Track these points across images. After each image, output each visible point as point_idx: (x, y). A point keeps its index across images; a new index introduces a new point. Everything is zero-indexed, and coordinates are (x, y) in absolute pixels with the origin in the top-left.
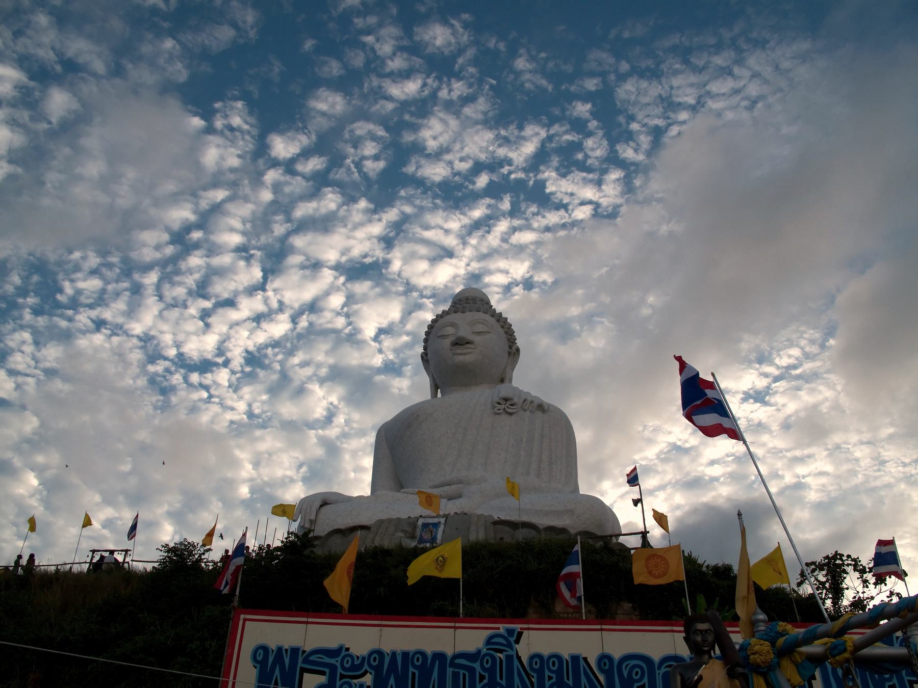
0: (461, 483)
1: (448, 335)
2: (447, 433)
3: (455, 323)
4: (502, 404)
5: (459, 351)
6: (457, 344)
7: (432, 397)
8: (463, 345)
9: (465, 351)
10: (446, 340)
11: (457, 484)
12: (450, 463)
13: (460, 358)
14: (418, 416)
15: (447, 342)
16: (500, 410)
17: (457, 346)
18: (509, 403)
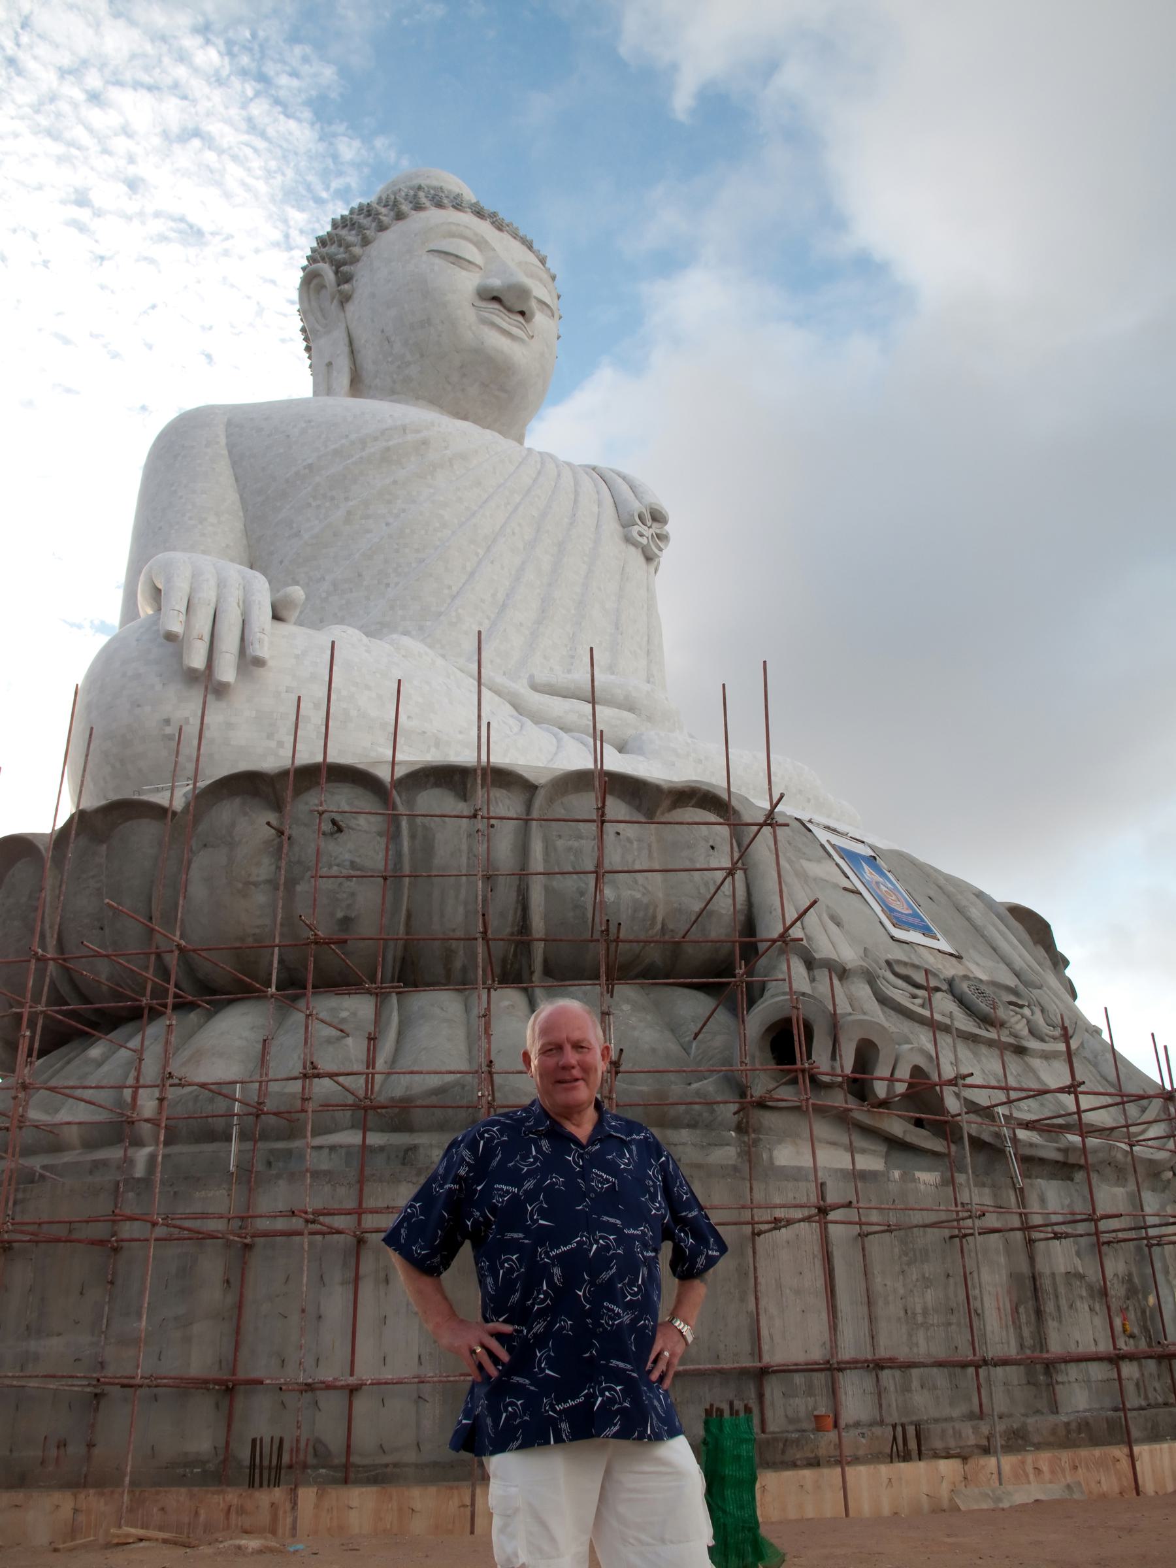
0: (631, 709)
1: (469, 262)
2: (514, 534)
3: (486, 242)
4: (644, 524)
5: (498, 320)
6: (496, 299)
7: (315, 393)
8: (510, 310)
9: (515, 331)
10: (464, 273)
11: (620, 706)
12: (521, 624)
13: (495, 341)
14: (425, 442)
15: (467, 282)
16: (641, 535)
17: (496, 306)
18: (656, 528)
